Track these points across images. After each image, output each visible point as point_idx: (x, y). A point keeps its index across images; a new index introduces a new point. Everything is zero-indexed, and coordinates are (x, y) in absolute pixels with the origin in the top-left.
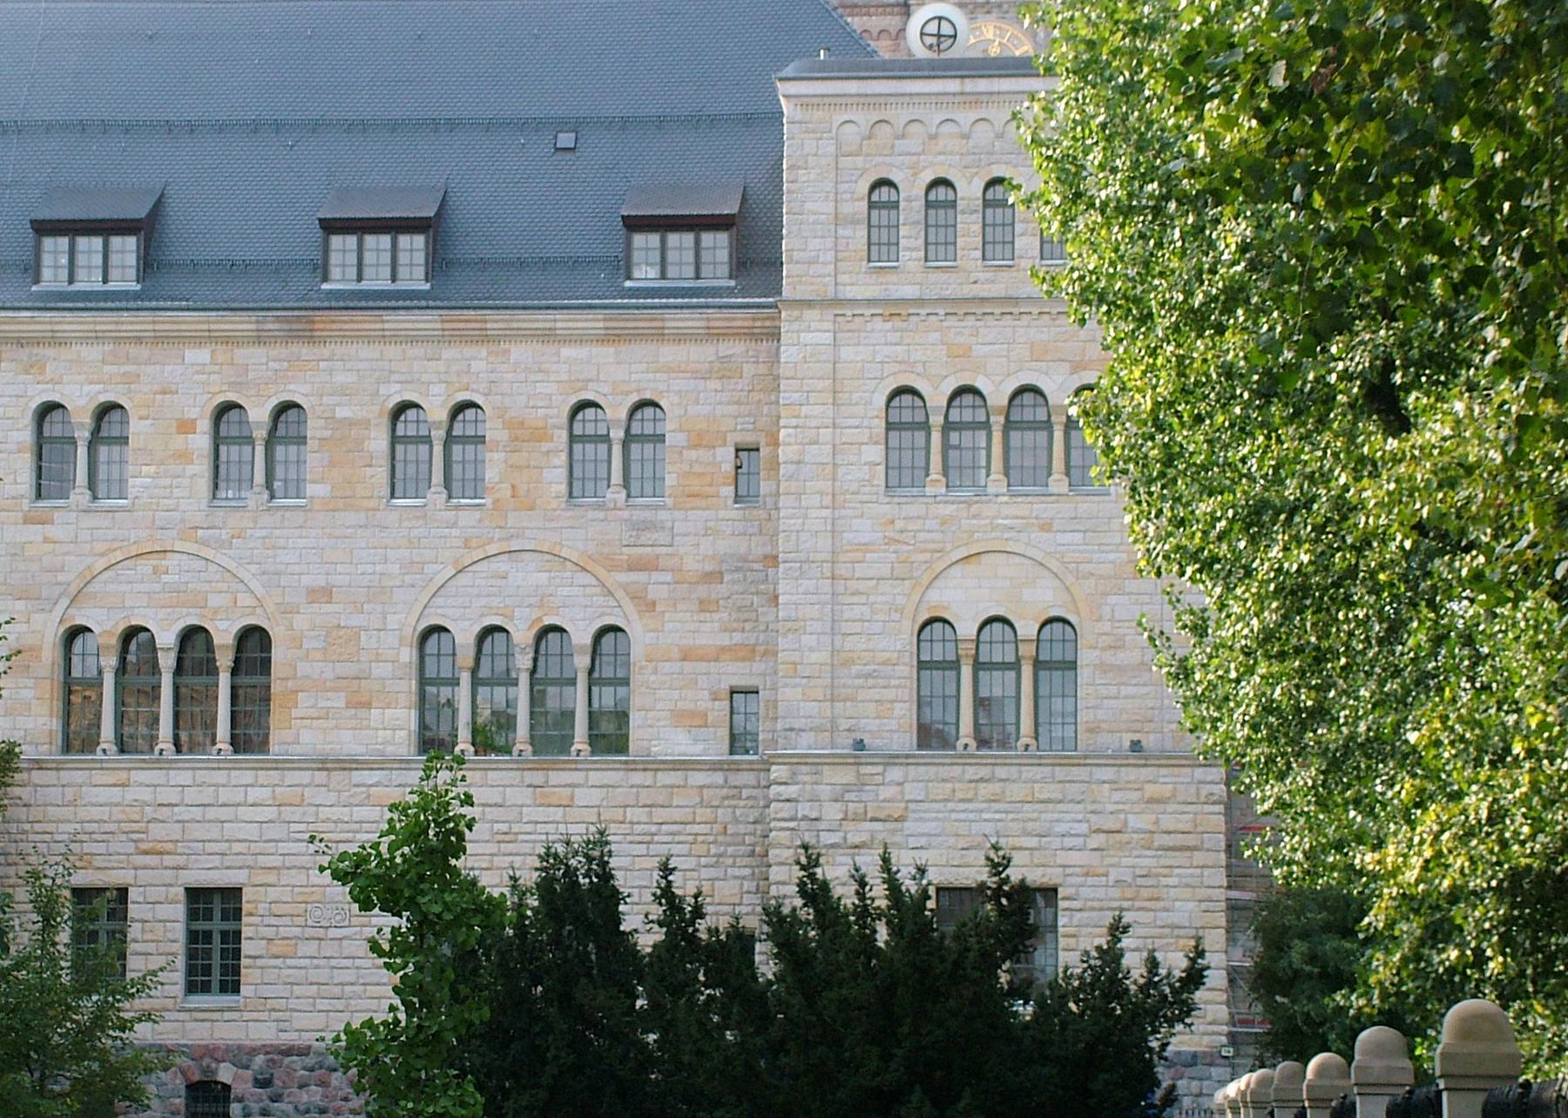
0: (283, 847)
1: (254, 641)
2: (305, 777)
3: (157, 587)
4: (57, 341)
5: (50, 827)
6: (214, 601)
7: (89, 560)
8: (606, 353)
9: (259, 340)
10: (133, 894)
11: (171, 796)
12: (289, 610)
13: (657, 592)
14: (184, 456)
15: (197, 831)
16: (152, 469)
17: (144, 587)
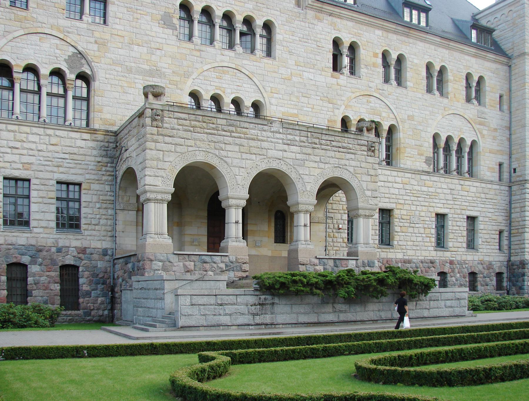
0: (405, 197)
1: (391, 130)
2: (409, 175)
3: (369, 107)
6: (384, 114)
8: (473, 60)
12: (403, 122)
13: (485, 132)
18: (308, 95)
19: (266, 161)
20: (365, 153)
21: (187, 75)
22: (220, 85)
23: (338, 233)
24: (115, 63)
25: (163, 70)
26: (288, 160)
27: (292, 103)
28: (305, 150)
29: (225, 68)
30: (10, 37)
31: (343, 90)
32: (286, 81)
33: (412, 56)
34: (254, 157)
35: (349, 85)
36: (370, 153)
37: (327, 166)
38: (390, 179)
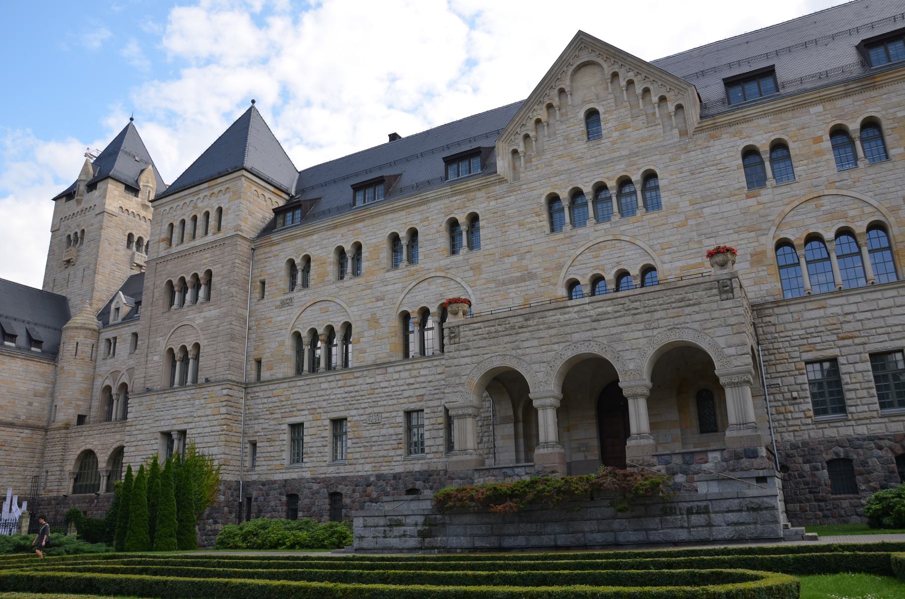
4: (746, 120)
5: (790, 333)
6: (851, 213)
7: (782, 208)
9: (847, 94)
10: (841, 360)
11: (853, 308)
14: (819, 153)
15: (870, 324)
16: (805, 162)
17: (813, 215)
18: (713, 235)
19: (572, 347)
20: (718, 298)
21: (560, 267)
22: (598, 263)
23: (793, 404)
24: (488, 281)
25: (534, 271)
26: (600, 339)
27: (692, 251)
28: (621, 321)
29: (601, 244)
30: (407, 290)
31: (769, 208)
32: (680, 229)
33: (891, 111)
34: (556, 347)
35: (777, 198)
36: (724, 296)
37: (656, 332)
38: (882, 303)
